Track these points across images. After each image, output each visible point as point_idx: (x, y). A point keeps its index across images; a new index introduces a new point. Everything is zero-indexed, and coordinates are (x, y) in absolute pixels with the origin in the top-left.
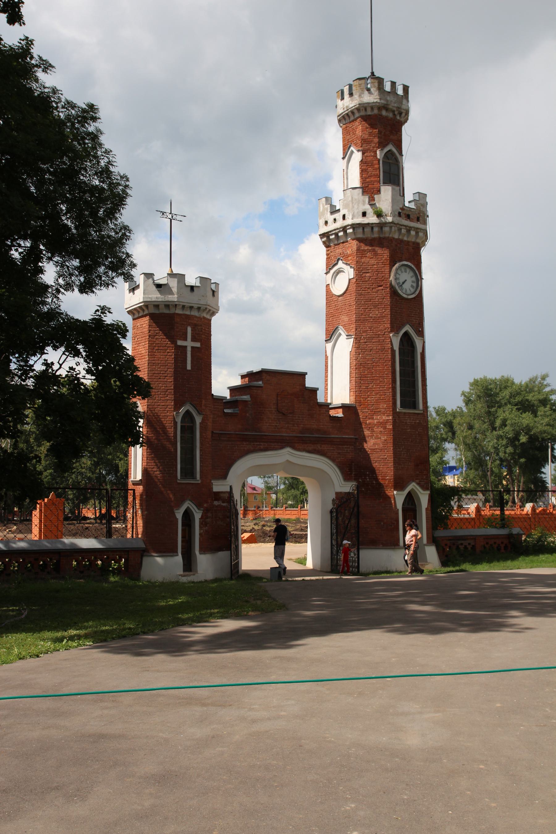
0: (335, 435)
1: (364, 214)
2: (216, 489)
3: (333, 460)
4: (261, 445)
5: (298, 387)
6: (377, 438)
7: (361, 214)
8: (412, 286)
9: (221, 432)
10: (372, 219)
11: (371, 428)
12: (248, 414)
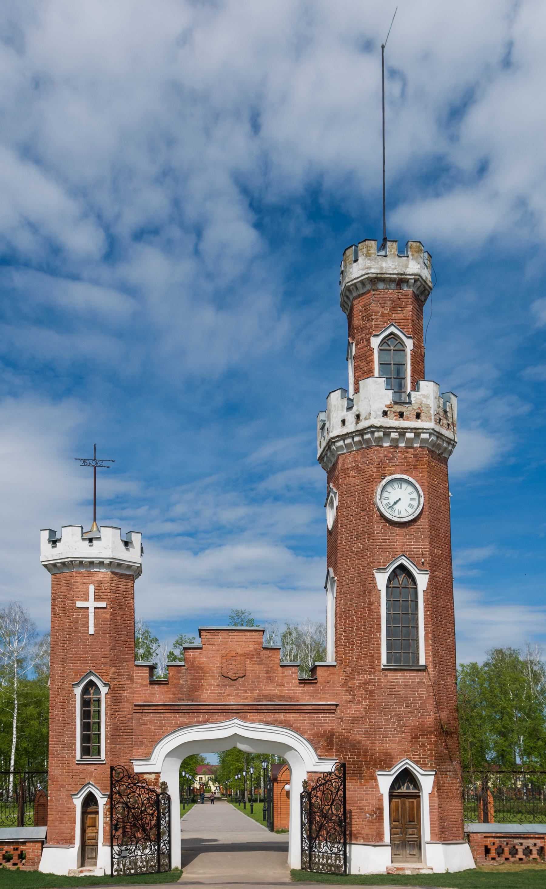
0: (306, 700)
1: (344, 422)
2: (138, 768)
3: (302, 734)
4: (198, 716)
5: (250, 646)
6: (359, 702)
7: (340, 423)
8: (411, 506)
9: (145, 704)
10: (351, 427)
11: (351, 691)
12: (181, 681)
